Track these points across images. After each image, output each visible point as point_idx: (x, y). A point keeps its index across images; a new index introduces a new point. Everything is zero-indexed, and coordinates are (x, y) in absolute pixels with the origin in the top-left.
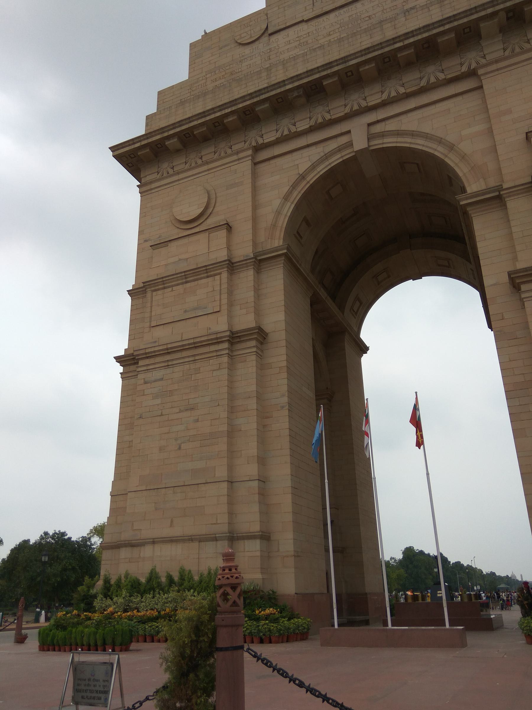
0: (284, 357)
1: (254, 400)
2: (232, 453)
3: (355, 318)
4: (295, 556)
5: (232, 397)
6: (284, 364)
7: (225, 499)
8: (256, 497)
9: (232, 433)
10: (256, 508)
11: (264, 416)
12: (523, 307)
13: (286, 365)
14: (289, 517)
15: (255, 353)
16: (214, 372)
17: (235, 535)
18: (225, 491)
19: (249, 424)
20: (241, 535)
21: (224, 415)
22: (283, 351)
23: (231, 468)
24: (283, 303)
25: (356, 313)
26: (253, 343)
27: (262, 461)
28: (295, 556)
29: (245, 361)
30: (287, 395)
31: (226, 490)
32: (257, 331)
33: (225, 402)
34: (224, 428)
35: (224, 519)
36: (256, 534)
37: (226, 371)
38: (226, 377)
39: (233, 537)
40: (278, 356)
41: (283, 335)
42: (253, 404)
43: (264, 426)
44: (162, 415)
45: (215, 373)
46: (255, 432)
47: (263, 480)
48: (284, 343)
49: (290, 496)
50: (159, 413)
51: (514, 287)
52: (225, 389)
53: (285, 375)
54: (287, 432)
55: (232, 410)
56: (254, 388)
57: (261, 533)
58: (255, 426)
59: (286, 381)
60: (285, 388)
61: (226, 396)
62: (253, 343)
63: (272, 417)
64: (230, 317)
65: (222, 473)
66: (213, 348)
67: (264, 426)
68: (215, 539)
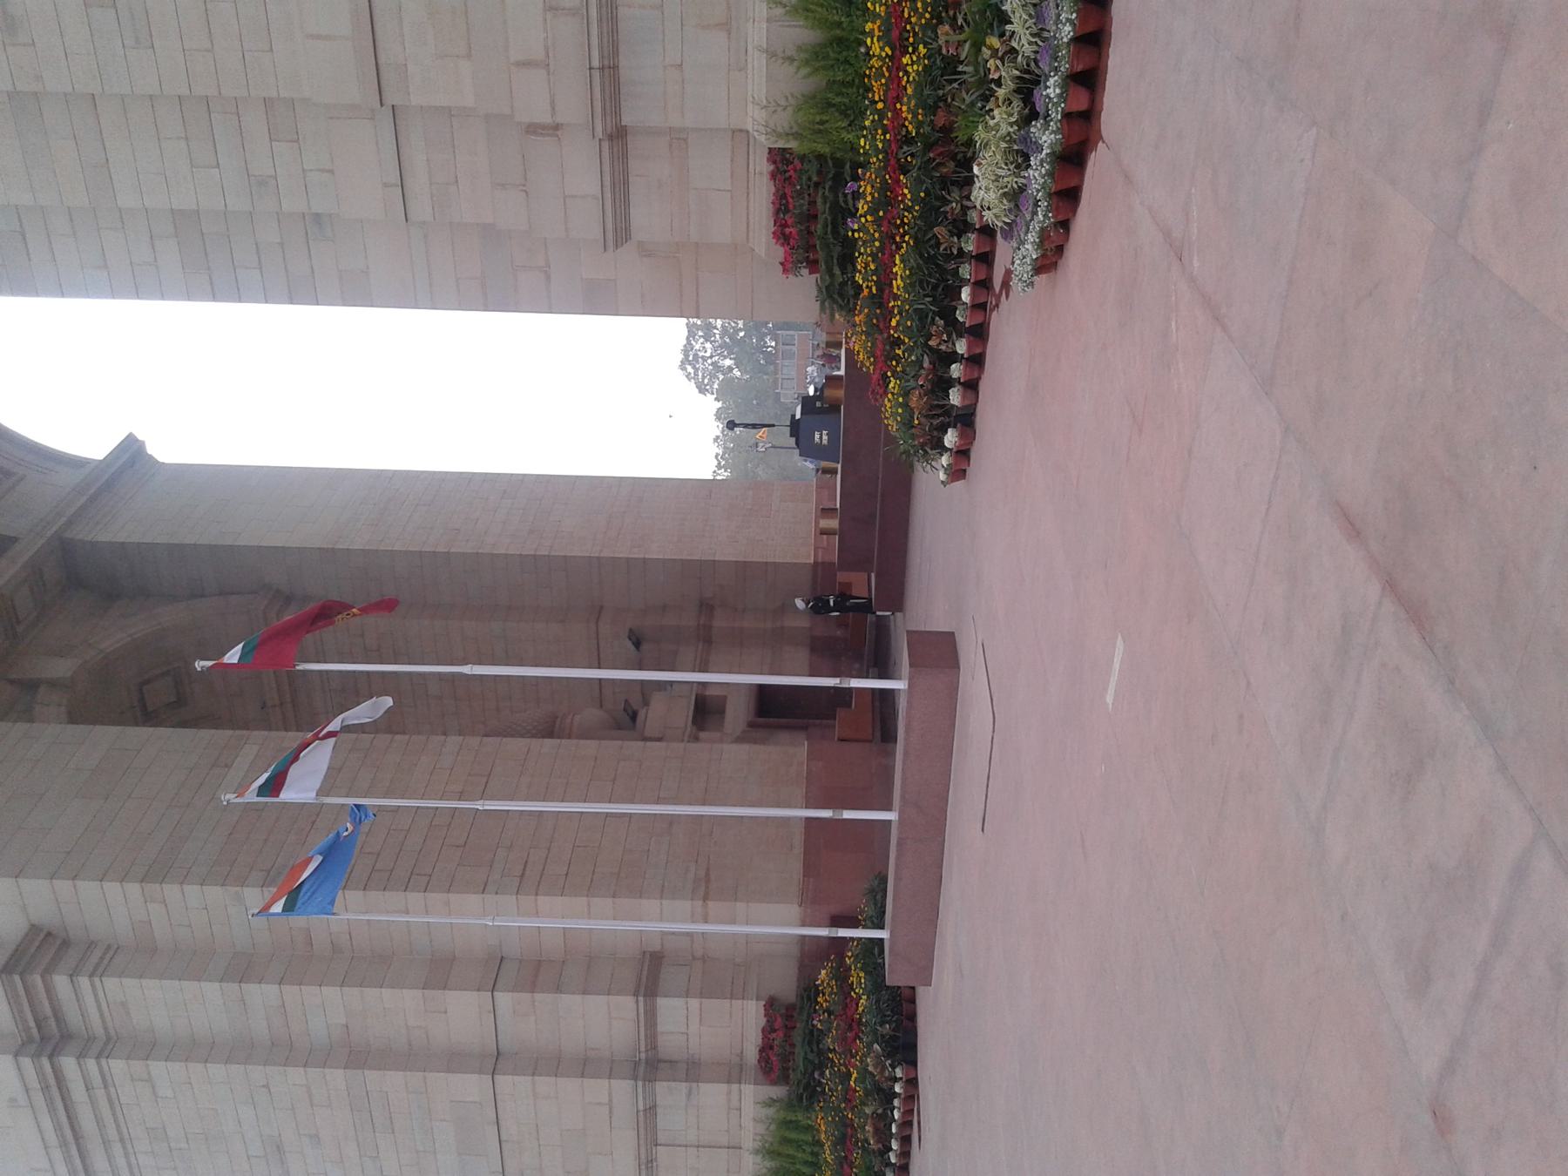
0: (112, 888)
1: (252, 989)
4: (705, 898)
6: (133, 889)
7: (545, 1083)
13: (137, 886)
17: (643, 1056)
18: (523, 1082)
20: (643, 1043)
21: (296, 1075)
22: (88, 888)
26: (61, 982)
28: (705, 898)
29: (123, 1004)
34: (337, 1076)
35: (598, 1088)
37: (158, 1068)
40: (105, 904)
42: (262, 995)
48: (64, 886)
53: (171, 891)
59: (192, 890)
60: (215, 893)
62: (61, 982)
65: (472, 1086)
68: (651, 1110)
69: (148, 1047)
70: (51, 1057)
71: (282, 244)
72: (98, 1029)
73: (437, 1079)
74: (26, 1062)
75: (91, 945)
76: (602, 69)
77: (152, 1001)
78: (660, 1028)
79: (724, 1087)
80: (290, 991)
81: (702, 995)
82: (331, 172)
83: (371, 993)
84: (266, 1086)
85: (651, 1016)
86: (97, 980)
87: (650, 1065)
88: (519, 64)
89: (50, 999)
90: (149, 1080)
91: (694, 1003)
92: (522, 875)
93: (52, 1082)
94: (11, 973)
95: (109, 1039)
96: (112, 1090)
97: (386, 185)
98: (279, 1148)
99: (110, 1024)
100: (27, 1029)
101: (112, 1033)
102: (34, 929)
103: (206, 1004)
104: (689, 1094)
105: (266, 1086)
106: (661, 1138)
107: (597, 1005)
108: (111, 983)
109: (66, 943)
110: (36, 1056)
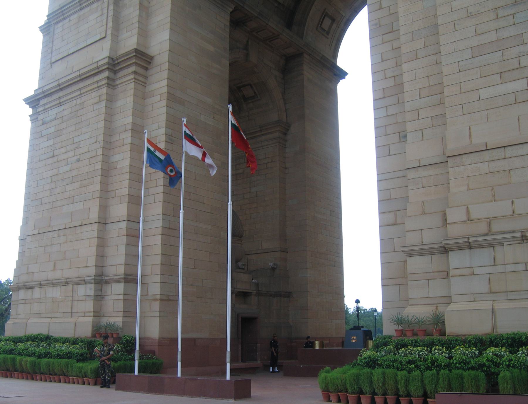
0: (165, 83)
1: (129, 134)
3: (327, 38)
4: (161, 300)
6: (165, 90)
7: (95, 241)
15: (133, 80)
17: (104, 278)
18: (95, 234)
22: (165, 74)
24: (169, 19)
25: (328, 33)
26: (133, 69)
28: (161, 300)
32: (134, 54)
35: (92, 261)
39: (102, 280)
42: (127, 137)
48: (166, 66)
53: (164, 103)
59: (164, 110)
60: (163, 117)
65: (94, 215)
68: (85, 283)
69: (110, 100)
70: (108, 68)
72: (118, 82)
74: (106, 60)
75: (146, 77)
76: (469, 242)
77: (126, 100)
79: (92, 310)
80: (128, 147)
81: (124, 300)
84: (96, 142)
86: (133, 80)
87: (101, 281)
89: (125, 66)
90: (100, 101)
91: (121, 297)
92: (169, 228)
93: (100, 69)
95: (114, 86)
96: (97, 89)
99: (119, 86)
100: (117, 60)
101: (117, 87)
103: (125, 119)
106: (75, 287)
107: (121, 260)
108: (132, 85)
109: (146, 69)
110: (108, 63)
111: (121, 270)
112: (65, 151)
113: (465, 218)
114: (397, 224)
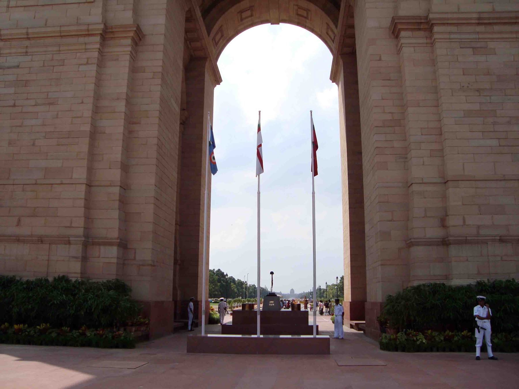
0: (160, 63)
2: (92, 156)
5: (97, 97)
6: (160, 69)
8: (117, 204)
9: (94, 134)
10: (115, 214)
11: (131, 120)
12: (399, 51)
14: (150, 227)
16: (81, 67)
19: (114, 126)
22: (160, 55)
23: (90, 170)
27: (125, 168)
29: (117, 60)
30: (158, 102)
31: (83, 193)
33: (91, 100)
34: (87, 128)
36: (114, 241)
37: (94, 68)
38: (94, 73)
41: (161, 39)
42: (121, 106)
43: (130, 132)
44: (14, 106)
45: (82, 68)
46: (121, 137)
47: (125, 187)
48: (161, 48)
49: (152, 206)
50: (11, 103)
51: (393, 33)
52: (92, 87)
54: (155, 141)
55: (97, 110)
56: (124, 89)
57: (119, 241)
58: (121, 129)
61: (92, 94)
63: (140, 124)
64: (105, 10)
66: (82, 40)
67: (130, 132)
69: (101, 64)
70: (101, 34)
71: (393, 147)
73: (85, 163)
78: (102, 247)
79: (79, 271)
80: (123, 116)
82: (423, 165)
83: (120, 143)
85: (111, 244)
88: (464, 217)
89: (122, 37)
90: (87, 63)
94: (137, 28)
97: (422, 179)
98: (50, 104)
101: (105, 54)
102: (144, 36)
104: (76, 258)
105: (82, 103)
106: (54, 247)
107: (115, 224)
108: (128, 57)
111: (114, 234)
112: (34, 104)
113: (462, 224)
114: (394, 221)
